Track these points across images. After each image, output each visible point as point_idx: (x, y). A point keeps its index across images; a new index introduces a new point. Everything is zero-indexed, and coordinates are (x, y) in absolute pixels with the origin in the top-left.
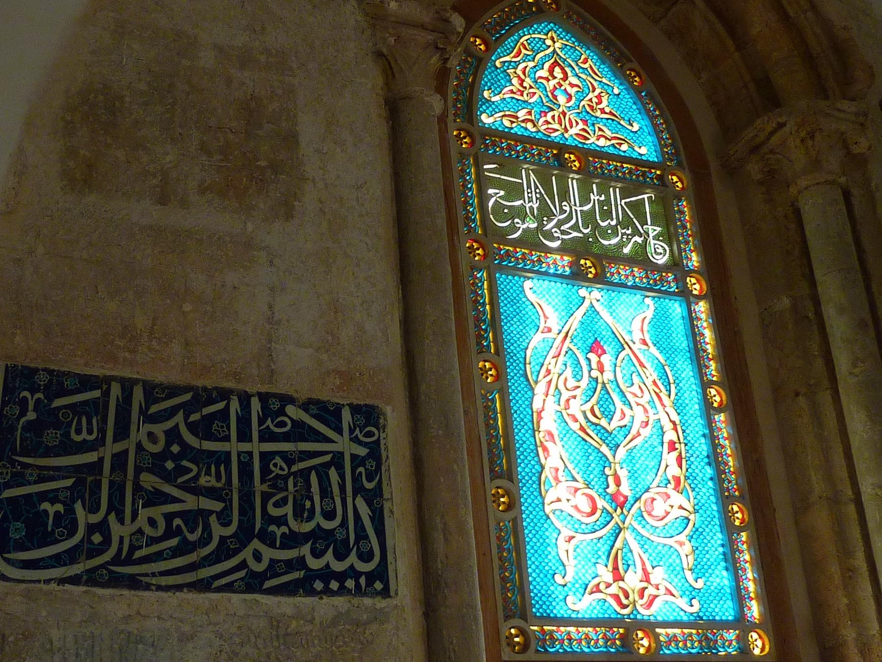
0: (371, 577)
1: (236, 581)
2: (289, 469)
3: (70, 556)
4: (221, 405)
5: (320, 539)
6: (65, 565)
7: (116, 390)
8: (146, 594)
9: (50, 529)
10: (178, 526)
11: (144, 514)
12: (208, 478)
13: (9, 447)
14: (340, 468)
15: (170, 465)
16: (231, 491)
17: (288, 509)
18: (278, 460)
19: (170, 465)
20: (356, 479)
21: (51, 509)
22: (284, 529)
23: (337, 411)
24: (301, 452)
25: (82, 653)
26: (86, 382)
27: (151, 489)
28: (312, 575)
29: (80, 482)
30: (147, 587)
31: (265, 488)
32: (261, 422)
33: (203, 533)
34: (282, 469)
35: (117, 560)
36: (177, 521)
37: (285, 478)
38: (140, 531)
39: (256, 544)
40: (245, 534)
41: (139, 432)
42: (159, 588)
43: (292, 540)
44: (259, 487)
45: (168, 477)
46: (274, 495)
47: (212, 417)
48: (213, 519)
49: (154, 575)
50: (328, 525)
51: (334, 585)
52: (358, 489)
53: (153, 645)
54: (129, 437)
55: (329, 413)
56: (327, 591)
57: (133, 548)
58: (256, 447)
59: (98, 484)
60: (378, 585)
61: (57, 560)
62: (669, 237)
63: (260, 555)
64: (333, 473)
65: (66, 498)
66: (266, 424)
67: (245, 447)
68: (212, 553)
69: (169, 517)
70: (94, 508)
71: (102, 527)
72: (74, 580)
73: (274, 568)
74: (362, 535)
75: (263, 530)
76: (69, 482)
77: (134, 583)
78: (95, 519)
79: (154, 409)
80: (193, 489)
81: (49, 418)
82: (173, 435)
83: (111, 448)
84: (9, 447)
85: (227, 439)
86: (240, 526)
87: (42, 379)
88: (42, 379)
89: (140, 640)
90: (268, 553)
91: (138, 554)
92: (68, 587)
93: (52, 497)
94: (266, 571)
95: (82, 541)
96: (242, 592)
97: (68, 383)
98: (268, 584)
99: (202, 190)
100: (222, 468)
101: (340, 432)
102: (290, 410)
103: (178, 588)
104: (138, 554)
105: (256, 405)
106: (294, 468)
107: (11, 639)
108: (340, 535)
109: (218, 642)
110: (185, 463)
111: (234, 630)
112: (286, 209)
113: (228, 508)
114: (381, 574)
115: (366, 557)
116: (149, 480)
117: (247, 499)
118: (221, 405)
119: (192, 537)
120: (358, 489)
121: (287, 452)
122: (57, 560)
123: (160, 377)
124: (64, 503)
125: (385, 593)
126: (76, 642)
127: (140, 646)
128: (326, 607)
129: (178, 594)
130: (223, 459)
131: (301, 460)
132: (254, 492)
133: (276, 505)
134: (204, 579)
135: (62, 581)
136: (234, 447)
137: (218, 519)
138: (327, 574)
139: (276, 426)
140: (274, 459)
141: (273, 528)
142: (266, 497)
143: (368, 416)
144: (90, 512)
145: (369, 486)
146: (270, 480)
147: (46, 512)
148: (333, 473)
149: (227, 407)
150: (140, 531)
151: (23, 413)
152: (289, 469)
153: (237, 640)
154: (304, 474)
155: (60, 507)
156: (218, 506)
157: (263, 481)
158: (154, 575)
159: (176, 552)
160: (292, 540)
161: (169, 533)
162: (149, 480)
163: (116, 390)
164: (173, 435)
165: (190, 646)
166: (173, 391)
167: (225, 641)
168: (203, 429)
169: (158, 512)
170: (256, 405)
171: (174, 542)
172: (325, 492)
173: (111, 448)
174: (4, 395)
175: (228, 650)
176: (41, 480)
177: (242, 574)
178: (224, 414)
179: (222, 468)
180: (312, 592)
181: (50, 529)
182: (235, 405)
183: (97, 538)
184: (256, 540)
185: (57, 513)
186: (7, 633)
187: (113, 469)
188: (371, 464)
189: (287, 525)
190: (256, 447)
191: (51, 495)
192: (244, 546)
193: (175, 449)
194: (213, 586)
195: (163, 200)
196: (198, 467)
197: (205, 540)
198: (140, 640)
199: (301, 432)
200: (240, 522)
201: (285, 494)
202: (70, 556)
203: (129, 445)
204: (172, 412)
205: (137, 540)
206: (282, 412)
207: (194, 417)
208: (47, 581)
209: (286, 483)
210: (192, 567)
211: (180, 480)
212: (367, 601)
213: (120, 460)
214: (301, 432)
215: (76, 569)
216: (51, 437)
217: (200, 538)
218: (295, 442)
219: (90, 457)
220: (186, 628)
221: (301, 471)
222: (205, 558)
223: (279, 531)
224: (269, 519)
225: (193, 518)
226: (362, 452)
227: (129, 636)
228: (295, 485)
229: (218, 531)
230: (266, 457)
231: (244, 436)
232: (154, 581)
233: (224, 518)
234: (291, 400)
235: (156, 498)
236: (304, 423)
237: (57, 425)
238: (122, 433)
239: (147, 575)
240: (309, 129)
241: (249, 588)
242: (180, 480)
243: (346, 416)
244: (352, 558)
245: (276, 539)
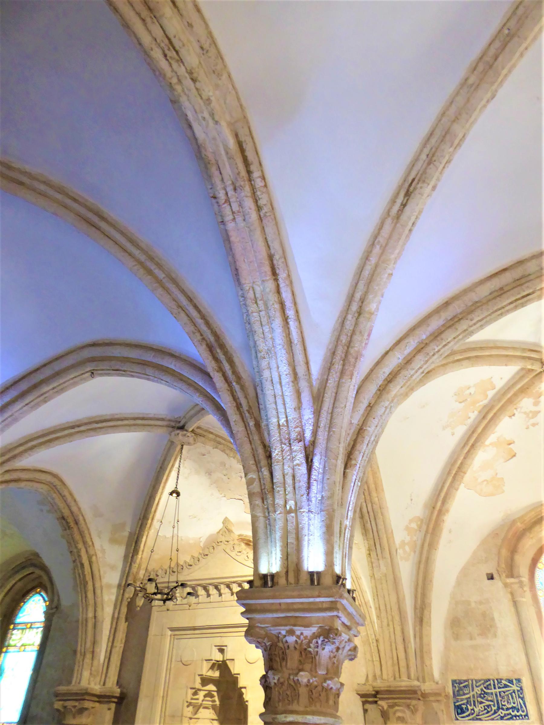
0: (525, 716)
3: (469, 715)
4: (489, 683)
5: (513, 708)
7: (470, 682)
11: (480, 706)
14: (514, 692)
15: (482, 696)
17: (506, 703)
19: (482, 696)
20: (518, 695)
21: (463, 706)
23: (512, 681)
26: (465, 681)
28: (513, 716)
29: (468, 701)
35: (477, 716)
39: (501, 710)
40: (499, 708)
41: (476, 689)
43: (508, 709)
44: (500, 699)
45: (483, 698)
47: (488, 686)
50: (514, 705)
51: (518, 718)
52: (519, 697)
55: (511, 681)
56: (516, 719)
58: (498, 690)
59: (470, 701)
60: (527, 717)
61: (467, 716)
63: (502, 713)
64: (513, 694)
67: (495, 690)
70: (471, 705)
71: (473, 709)
72: (470, 720)
73: (505, 715)
74: (521, 707)
77: (480, 719)
78: (472, 708)
79: (477, 685)
80: (487, 700)
81: (460, 689)
82: (482, 690)
83: (472, 693)
87: (458, 681)
88: (458, 681)
90: (504, 712)
91: (480, 714)
93: (464, 704)
99: (478, 635)
101: (513, 685)
102: (503, 681)
103: (488, 720)
105: (496, 682)
108: (517, 707)
112: (495, 636)
113: (494, 704)
114: (527, 715)
115: (523, 711)
118: (489, 683)
119: (489, 710)
120: (519, 697)
122: (467, 716)
123: (476, 678)
125: (528, 719)
136: (493, 691)
138: (516, 716)
142: (501, 701)
143: (519, 680)
145: (521, 696)
148: (513, 694)
154: (508, 695)
155: (465, 706)
156: (492, 703)
159: (487, 713)
160: (508, 709)
161: (485, 709)
162: (479, 699)
163: (470, 682)
164: (482, 690)
166: (480, 681)
169: (482, 705)
170: (496, 682)
172: (512, 698)
173: (472, 693)
178: (490, 684)
180: (513, 720)
182: (492, 682)
188: (521, 691)
190: (498, 690)
195: (471, 639)
197: (491, 710)
199: (506, 686)
202: (469, 715)
203: (474, 692)
204: (480, 685)
207: (485, 685)
210: (490, 716)
212: (525, 721)
213: (473, 696)
214: (506, 686)
215: (471, 717)
216: (461, 692)
219: (468, 696)
223: (505, 707)
224: (503, 705)
225: (488, 706)
226: (519, 689)
229: (494, 708)
230: (500, 692)
231: (495, 688)
233: (494, 706)
235: (481, 703)
237: (462, 690)
238: (473, 690)
240: (496, 616)
241: (501, 719)
243: (514, 681)
244: (520, 712)
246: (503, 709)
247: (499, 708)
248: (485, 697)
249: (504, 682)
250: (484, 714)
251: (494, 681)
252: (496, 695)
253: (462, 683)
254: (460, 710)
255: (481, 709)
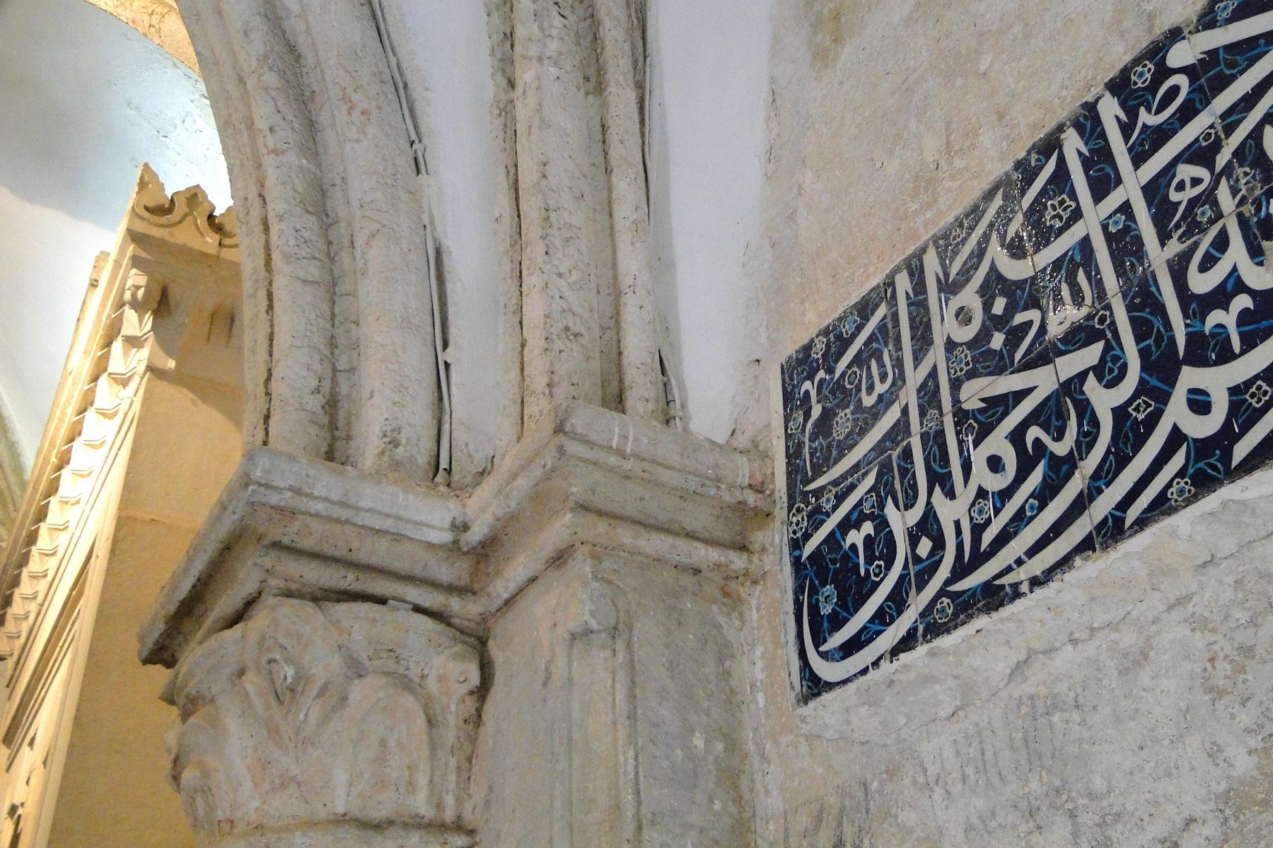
1: (1169, 485)
2: (1210, 166)
6: (892, 621)
8: (1019, 605)
9: (862, 573)
10: (1037, 441)
12: (1060, 315)
13: (799, 478)
16: (1108, 307)
17: (1237, 252)
18: (1186, 171)
21: (855, 538)
22: (1243, 302)
24: (1224, 116)
25: (970, 771)
26: (864, 309)
27: (983, 405)
30: (1016, 594)
31: (1175, 247)
32: (1126, 129)
33: (1080, 425)
34: (1196, 182)
35: (961, 570)
36: (1034, 432)
37: (1209, 197)
38: (982, 493)
39: (1190, 377)
41: (946, 327)
42: (1035, 582)
44: (1158, 255)
45: (1001, 365)
46: (1196, 245)
48: (1092, 387)
49: (1019, 562)
53: (1077, 707)
54: (932, 343)
57: (978, 530)
59: (907, 454)
61: (883, 618)
65: (873, 507)
66: (1139, 125)
67: (1114, 200)
68: (1108, 452)
69: (1017, 437)
72: (906, 643)
75: (1195, 339)
76: (870, 480)
77: (994, 596)
84: (799, 478)
85: (1077, 215)
86: (1143, 369)
89: (1055, 705)
90: (1217, 381)
91: (988, 537)
92: (904, 657)
94: (1227, 425)
95: (906, 567)
96: (1188, 502)
97: (847, 329)
98: (1241, 450)
100: (1081, 278)
103: (1064, 563)
104: (988, 537)
106: (1222, 159)
107: (875, 784)
109: (1199, 641)
110: (1019, 318)
111: (1228, 595)
116: (975, 393)
117: (1144, 302)
121: (1197, 140)
122: (883, 618)
124: (871, 517)
126: (958, 754)
127: (1056, 718)
129: (1067, 577)
130: (1078, 258)
131: (1229, 129)
132: (1153, 274)
133: (1208, 263)
134: (1106, 519)
135: (895, 651)
137: (1100, 378)
139: (1160, 109)
140: (1174, 176)
141: (1215, 317)
144: (906, 509)
146: (1178, 226)
147: (853, 547)
149: (1062, 161)
150: (982, 493)
151: (807, 415)
152: (1210, 166)
153: (1241, 616)
156: (1091, 354)
157: (1164, 237)
158: (1019, 562)
159: (1045, 495)
164: (995, 283)
165: (1145, 678)
167: (1214, 630)
170: (1110, 110)
171: (1036, 478)
174: (785, 410)
175: (1228, 650)
176: (840, 498)
177: (1178, 460)
179: (1081, 278)
181: (862, 573)
182: (1073, 144)
183: (925, 546)
184: (1186, 370)
185: (868, 540)
186: (869, 776)
187: (923, 414)
189: (1241, 287)
191: (854, 517)
192: (1163, 398)
193: (999, 306)
194: (1128, 524)
196: (1040, 308)
197: (1087, 441)
198: (1055, 705)
200: (1144, 354)
201: (1214, 231)
203: (937, 355)
204: (980, 253)
205: (980, 512)
206: (1163, 72)
208: (876, 664)
209: (1215, 203)
211: (1018, 355)
216: (843, 422)
217: (1078, 442)
218: (1208, 103)
219: (893, 414)
220: (1128, 639)
221: (1239, 154)
222: (1096, 476)
223: (1225, 318)
224: (1196, 306)
227: (1033, 706)
228: (1234, 191)
229: (1104, 400)
232: (1022, 575)
233: (1109, 371)
234: (1175, 35)
236: (1213, 53)
239: (1009, 569)
242: (1018, 355)
245: (1228, 339)
246: (1208, 350)
248: (1015, 336)
249: (1179, 56)
250: (1021, 519)
251: (1088, 121)
252: (1125, 244)
253: (845, 343)
255: (995, 483)
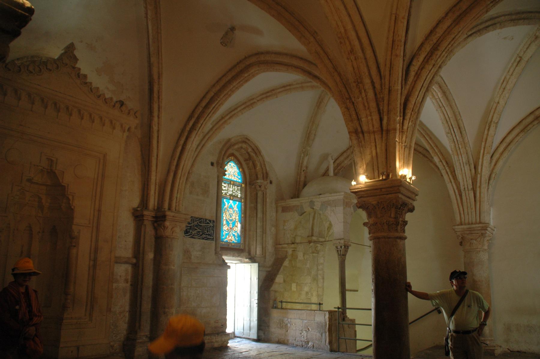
5: (209, 234)
40: (203, 234)
55: (210, 221)
58: (204, 225)
62: (241, 193)
63: (204, 236)
73: (205, 237)
77: (194, 238)
128: (208, 241)
136: (202, 224)
160: (206, 235)
168: (200, 223)
190: (204, 225)
225: (199, 232)
247: (203, 234)
254: (186, 232)
